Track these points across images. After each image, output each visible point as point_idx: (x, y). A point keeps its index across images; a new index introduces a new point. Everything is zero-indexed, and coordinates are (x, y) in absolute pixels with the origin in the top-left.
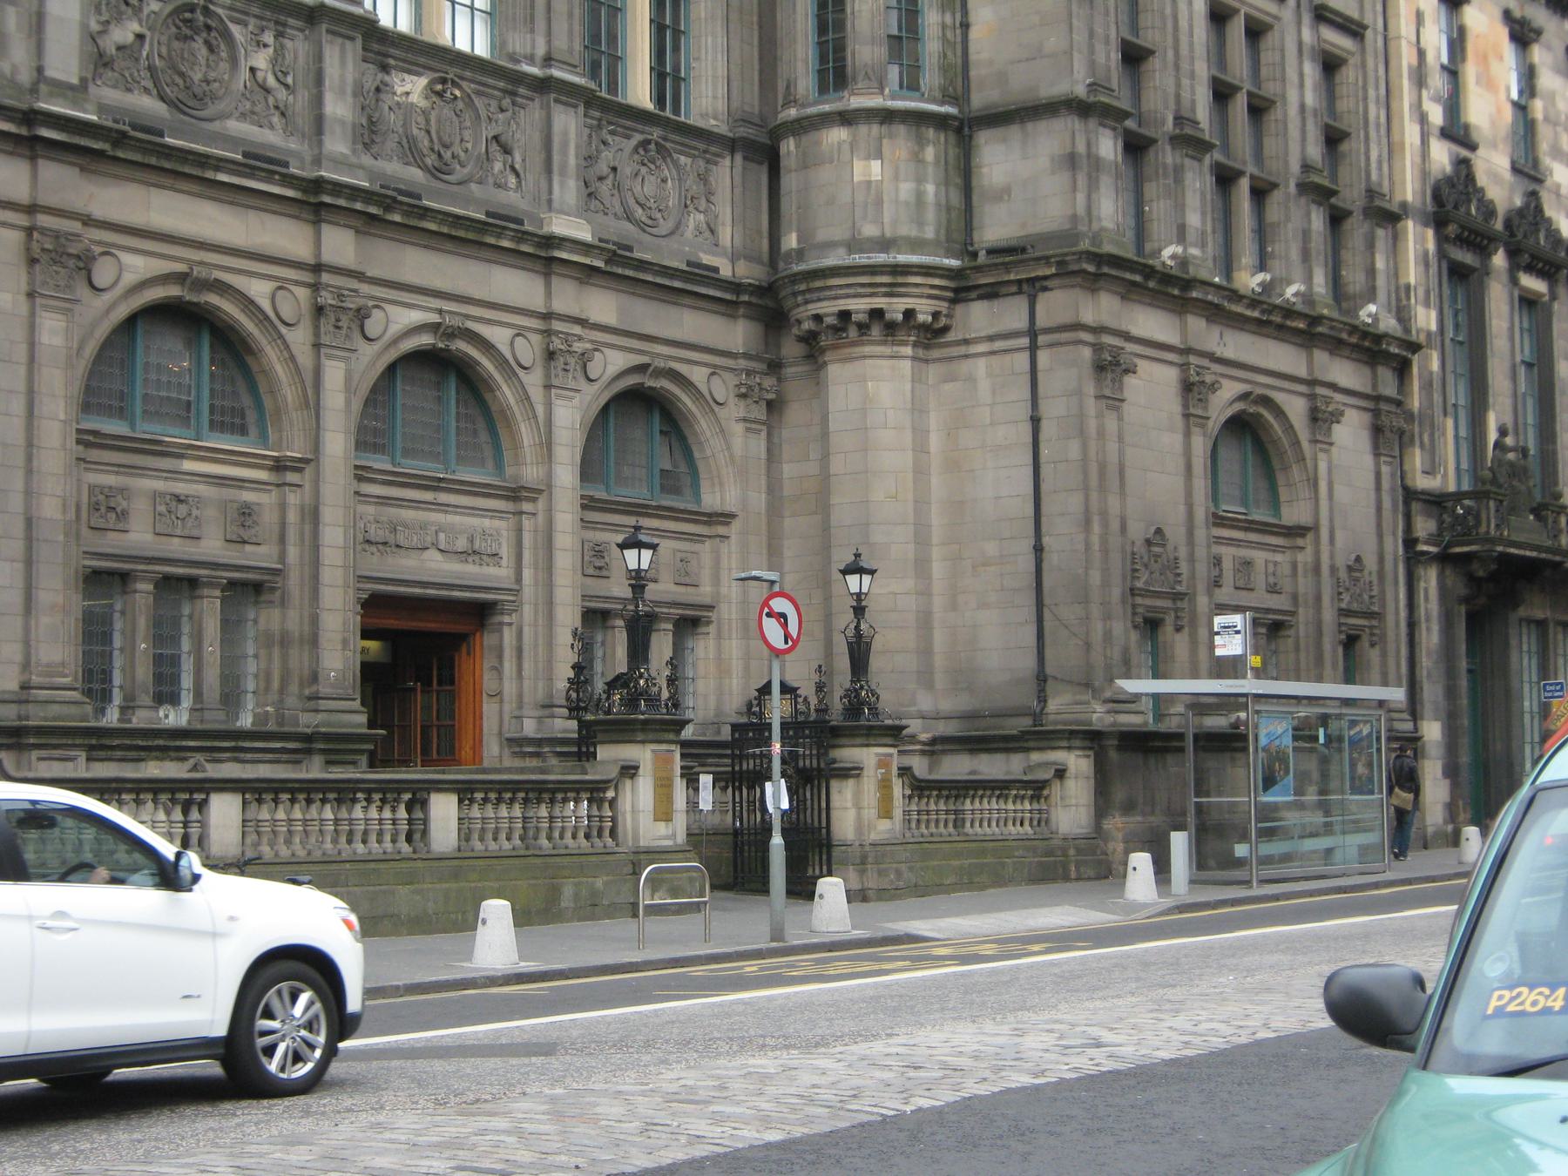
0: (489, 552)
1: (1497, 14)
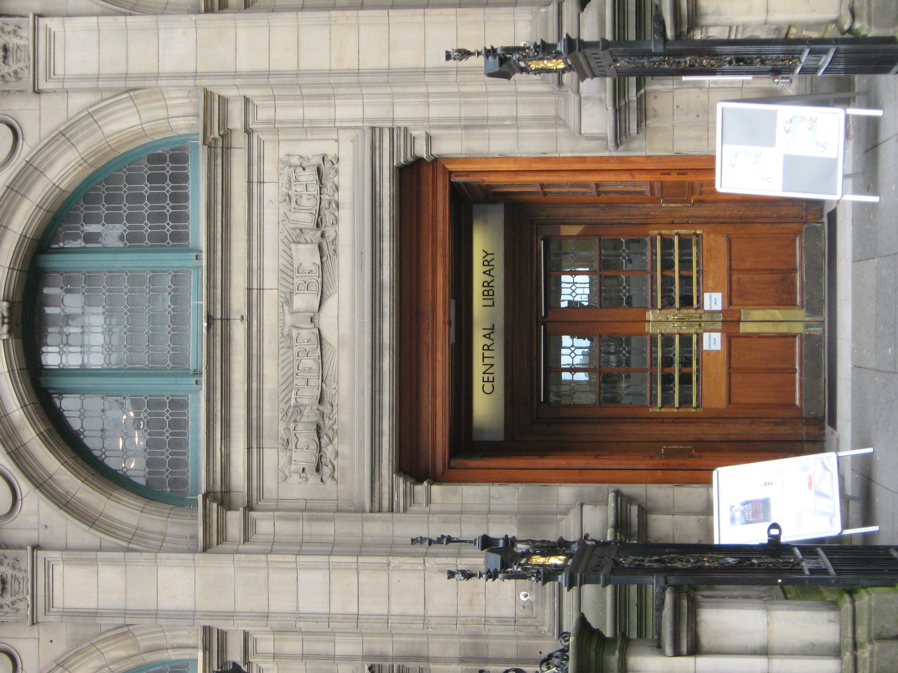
0: (314, 189)
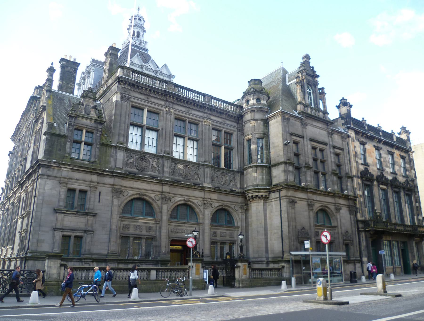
1: (372, 146)
